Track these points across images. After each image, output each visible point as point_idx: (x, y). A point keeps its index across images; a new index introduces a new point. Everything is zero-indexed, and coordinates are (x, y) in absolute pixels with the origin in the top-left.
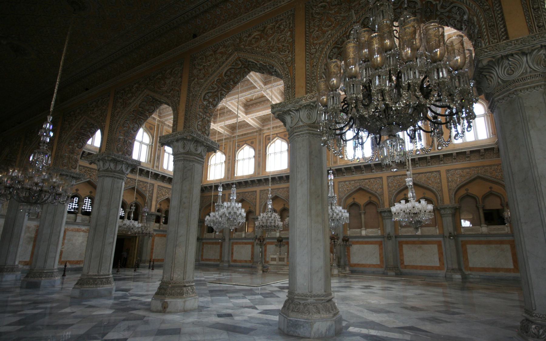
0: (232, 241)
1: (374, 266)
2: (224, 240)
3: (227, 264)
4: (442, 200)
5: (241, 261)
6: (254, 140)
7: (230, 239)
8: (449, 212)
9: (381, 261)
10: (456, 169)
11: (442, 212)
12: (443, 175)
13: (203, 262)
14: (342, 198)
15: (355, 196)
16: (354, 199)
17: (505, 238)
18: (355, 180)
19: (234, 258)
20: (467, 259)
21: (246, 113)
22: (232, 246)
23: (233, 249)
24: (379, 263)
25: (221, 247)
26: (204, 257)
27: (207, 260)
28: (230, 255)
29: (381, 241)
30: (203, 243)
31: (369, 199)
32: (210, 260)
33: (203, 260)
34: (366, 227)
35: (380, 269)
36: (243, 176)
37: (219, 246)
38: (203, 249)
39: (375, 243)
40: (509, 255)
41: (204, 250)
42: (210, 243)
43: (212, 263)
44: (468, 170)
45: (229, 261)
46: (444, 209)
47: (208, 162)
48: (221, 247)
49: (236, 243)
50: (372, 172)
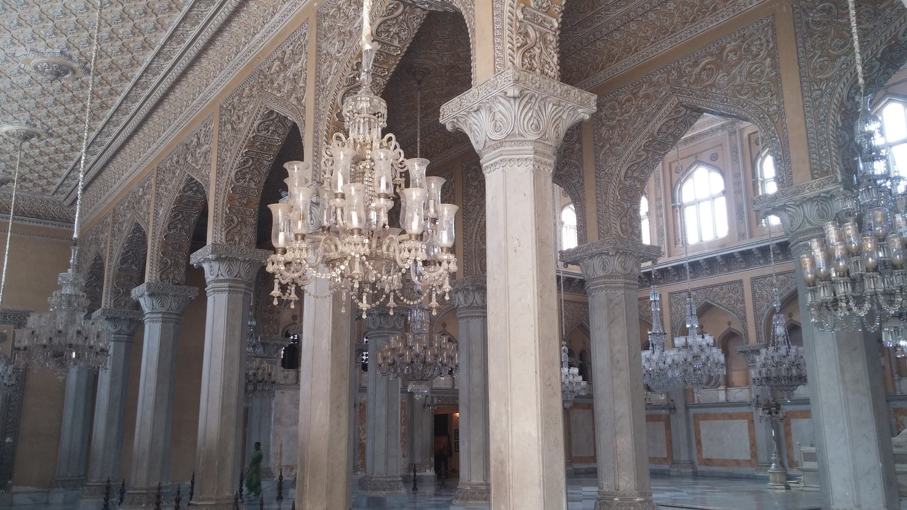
0: (692, 411)
5: (724, 463)
7: (687, 408)
19: (706, 454)
22: (697, 425)
23: (698, 433)
25: (668, 426)
45: (692, 463)
48: (668, 426)
49: (707, 417)
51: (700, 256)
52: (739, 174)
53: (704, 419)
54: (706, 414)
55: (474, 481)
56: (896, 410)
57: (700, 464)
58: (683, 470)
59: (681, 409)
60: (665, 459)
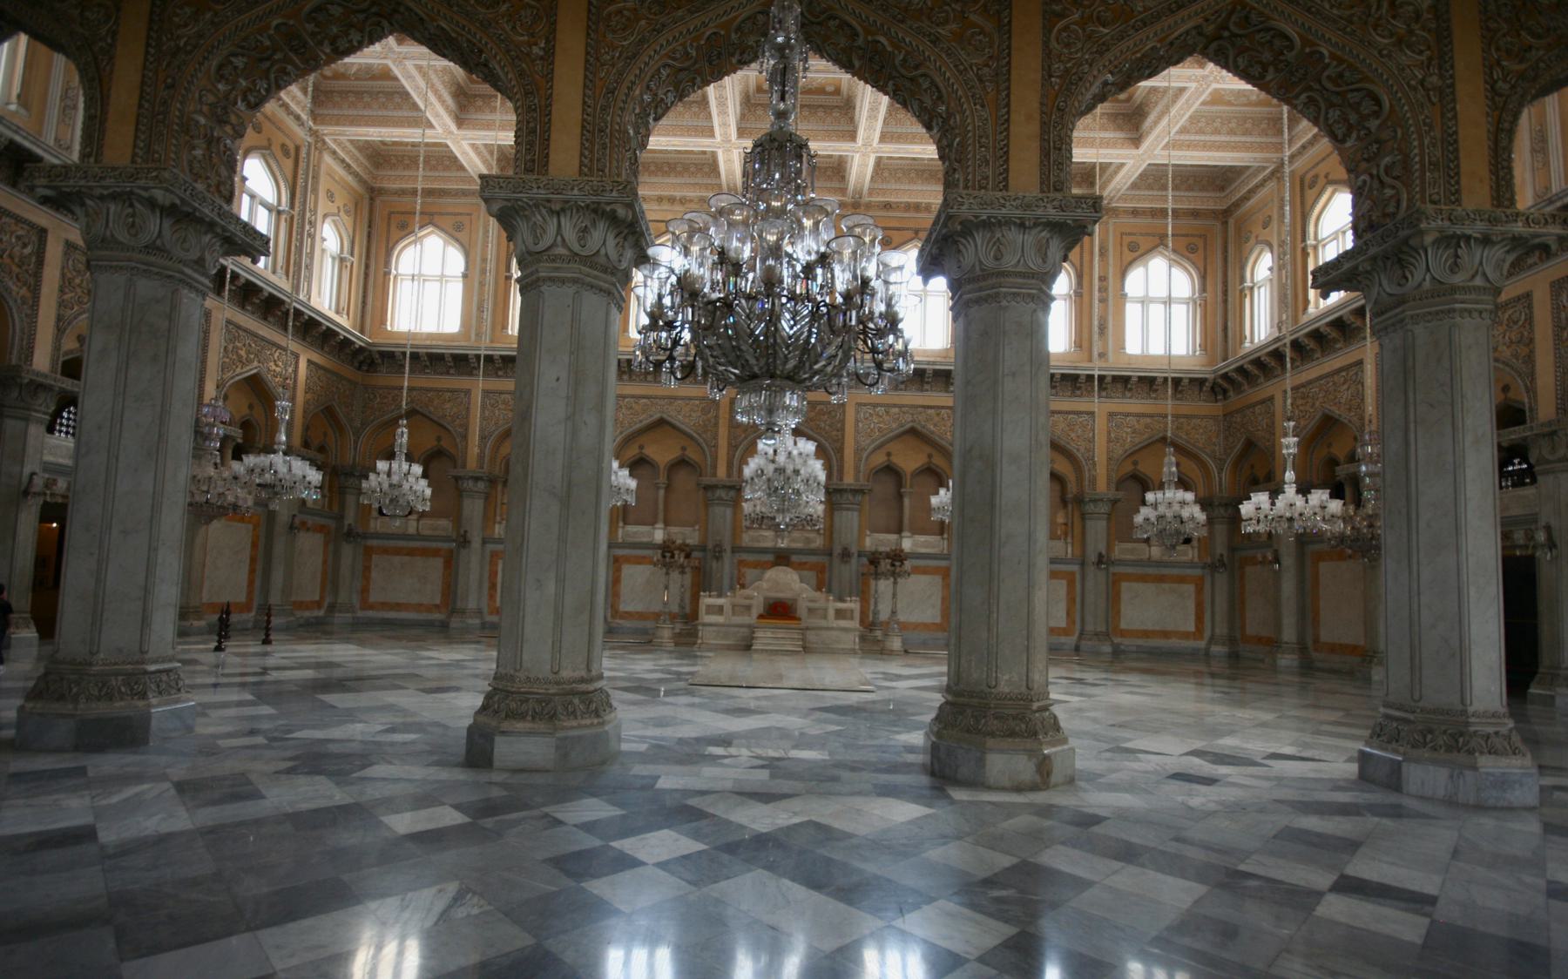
0: (490, 547)
1: (926, 626)
2: (464, 542)
4: (1093, 481)
6: (465, 220)
7: (484, 542)
8: (1104, 508)
9: (945, 613)
10: (1128, 415)
11: (1090, 508)
12: (1101, 424)
13: (371, 614)
14: (864, 449)
15: (891, 447)
16: (889, 454)
17: (1189, 572)
18: (900, 406)
20: (1119, 612)
21: (460, 122)
24: (938, 620)
26: (374, 597)
27: (385, 606)
30: (369, 552)
32: (398, 606)
33: (367, 606)
34: (916, 531)
35: (940, 635)
36: (414, 336)
37: (438, 563)
38: (367, 569)
40: (1191, 605)
41: (374, 574)
42: (398, 552)
44: (1148, 420)
45: (479, 612)
46: (1095, 501)
51: (447, 348)
55: (566, 674)
58: (470, 621)
59: (476, 543)
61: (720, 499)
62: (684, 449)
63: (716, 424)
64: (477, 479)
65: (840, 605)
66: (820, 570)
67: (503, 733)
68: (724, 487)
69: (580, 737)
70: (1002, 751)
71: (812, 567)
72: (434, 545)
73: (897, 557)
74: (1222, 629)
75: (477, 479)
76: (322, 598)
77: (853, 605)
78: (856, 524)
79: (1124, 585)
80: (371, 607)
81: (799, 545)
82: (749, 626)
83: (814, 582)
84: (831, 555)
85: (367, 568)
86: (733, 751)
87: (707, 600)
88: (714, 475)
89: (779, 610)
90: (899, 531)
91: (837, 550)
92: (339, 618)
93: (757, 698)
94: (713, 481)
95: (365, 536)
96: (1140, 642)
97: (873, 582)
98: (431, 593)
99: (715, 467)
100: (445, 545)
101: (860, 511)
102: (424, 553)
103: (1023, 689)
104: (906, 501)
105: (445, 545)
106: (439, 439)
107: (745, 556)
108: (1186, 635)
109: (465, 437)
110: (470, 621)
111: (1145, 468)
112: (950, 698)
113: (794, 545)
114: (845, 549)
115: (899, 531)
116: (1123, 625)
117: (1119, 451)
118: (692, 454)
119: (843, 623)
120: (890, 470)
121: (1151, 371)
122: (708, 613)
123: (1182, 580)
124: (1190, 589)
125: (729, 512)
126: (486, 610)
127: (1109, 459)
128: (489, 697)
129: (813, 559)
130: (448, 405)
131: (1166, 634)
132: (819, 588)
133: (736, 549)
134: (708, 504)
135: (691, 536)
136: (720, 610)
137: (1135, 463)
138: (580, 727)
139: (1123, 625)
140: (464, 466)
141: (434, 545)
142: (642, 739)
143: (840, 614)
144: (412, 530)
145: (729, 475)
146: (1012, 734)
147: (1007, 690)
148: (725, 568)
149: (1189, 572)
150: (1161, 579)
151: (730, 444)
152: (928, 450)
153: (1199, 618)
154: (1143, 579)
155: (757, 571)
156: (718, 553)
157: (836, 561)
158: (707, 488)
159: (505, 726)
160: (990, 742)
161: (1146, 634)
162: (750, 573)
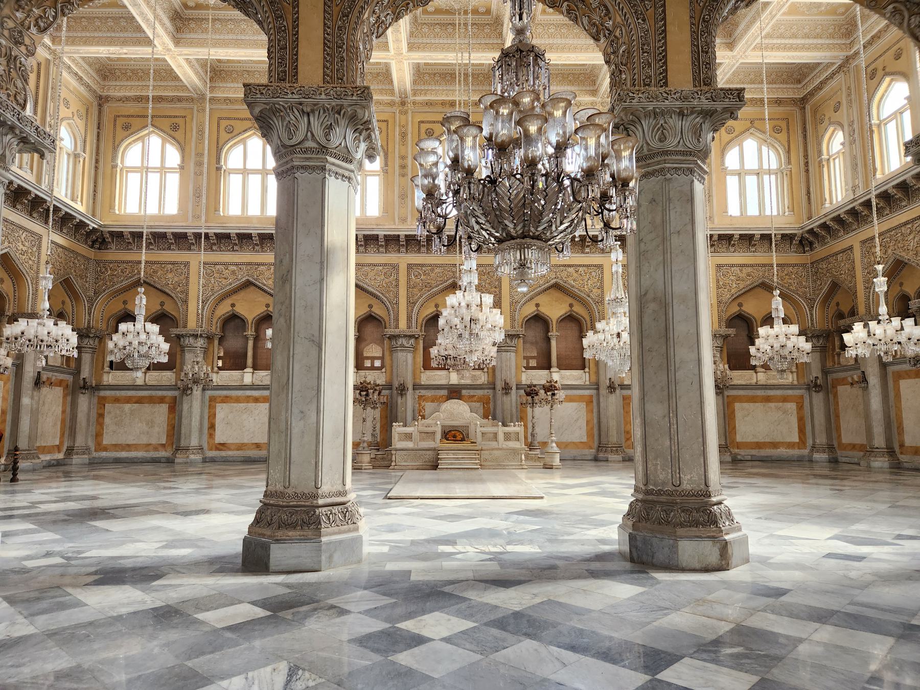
3: (197, 457)
5: (241, 447)
9: (590, 434)
10: (732, 266)
13: (104, 454)
15: (540, 299)
16: (537, 305)
19: (219, 438)
22: (212, 407)
24: (585, 439)
26: (106, 442)
27: (117, 447)
28: (206, 431)
29: (591, 396)
30: (102, 402)
31: (568, 308)
32: (128, 447)
37: (164, 408)
39: (580, 399)
41: (107, 420)
42: (128, 400)
43: (140, 454)
44: (749, 270)
47: (114, 158)
49: (226, 400)
50: (583, 252)
52: (202, 154)
53: (223, 401)
54: (227, 397)
56: (420, 397)
57: (211, 450)
58: (192, 457)
60: (163, 445)
61: (402, 346)
62: (370, 306)
63: (397, 286)
64: (196, 336)
65: (507, 429)
66: (485, 401)
67: (278, 541)
68: (405, 336)
69: (341, 542)
70: (690, 538)
71: (480, 400)
72: (160, 393)
73: (550, 388)
74: (821, 439)
75: (196, 336)
76: (62, 442)
77: (516, 428)
78: (513, 364)
79: (737, 405)
80: (105, 449)
81: (468, 382)
82: (434, 449)
83: (481, 411)
84: (494, 388)
85: (101, 416)
86: (459, 548)
87: (398, 429)
88: (397, 327)
89: (454, 434)
90: (549, 367)
91: (499, 385)
92: (76, 459)
93: (460, 506)
94: (397, 332)
95: (98, 387)
96: (754, 452)
97: (529, 410)
98: (159, 434)
99: (397, 320)
100: (170, 393)
101: (516, 352)
102: (151, 400)
103: (703, 486)
104: (554, 343)
105: (170, 393)
106: (162, 304)
107: (423, 392)
108: (790, 445)
109: (185, 302)
110: (192, 457)
111: (751, 308)
112: (640, 496)
113: (463, 382)
114: (506, 384)
115: (549, 367)
116: (739, 439)
117: (727, 296)
118: (378, 310)
119: (512, 444)
120: (539, 320)
121: (750, 229)
122: (400, 440)
123: (785, 399)
124: (792, 406)
125: (410, 356)
126: (205, 446)
127: (720, 302)
128: (260, 512)
129: (480, 393)
130: (170, 275)
131: (775, 445)
132: (485, 416)
133: (416, 387)
134: (392, 350)
135: (379, 378)
136: (409, 437)
137: (740, 305)
138: (340, 533)
139: (739, 439)
140: (185, 327)
141: (160, 393)
142: (383, 543)
143: (507, 437)
144: (140, 382)
145: (409, 327)
146: (696, 524)
147: (689, 487)
148: (409, 401)
149: (790, 392)
150: (768, 399)
151: (408, 302)
152: (570, 300)
153: (802, 430)
154: (753, 399)
155: (435, 405)
156: (402, 390)
157: (499, 393)
158: (392, 337)
159: (279, 534)
160: (680, 531)
161: (759, 445)
162: (429, 406)
